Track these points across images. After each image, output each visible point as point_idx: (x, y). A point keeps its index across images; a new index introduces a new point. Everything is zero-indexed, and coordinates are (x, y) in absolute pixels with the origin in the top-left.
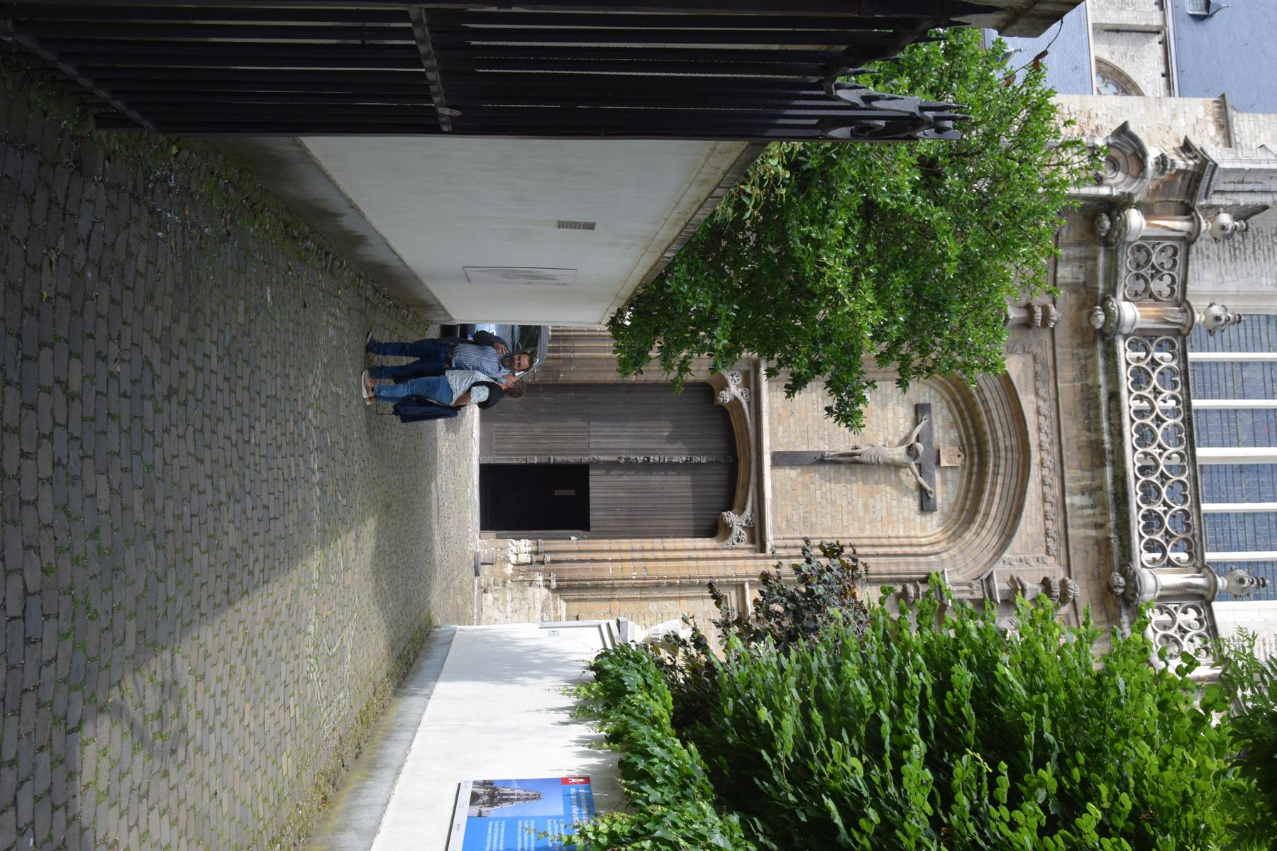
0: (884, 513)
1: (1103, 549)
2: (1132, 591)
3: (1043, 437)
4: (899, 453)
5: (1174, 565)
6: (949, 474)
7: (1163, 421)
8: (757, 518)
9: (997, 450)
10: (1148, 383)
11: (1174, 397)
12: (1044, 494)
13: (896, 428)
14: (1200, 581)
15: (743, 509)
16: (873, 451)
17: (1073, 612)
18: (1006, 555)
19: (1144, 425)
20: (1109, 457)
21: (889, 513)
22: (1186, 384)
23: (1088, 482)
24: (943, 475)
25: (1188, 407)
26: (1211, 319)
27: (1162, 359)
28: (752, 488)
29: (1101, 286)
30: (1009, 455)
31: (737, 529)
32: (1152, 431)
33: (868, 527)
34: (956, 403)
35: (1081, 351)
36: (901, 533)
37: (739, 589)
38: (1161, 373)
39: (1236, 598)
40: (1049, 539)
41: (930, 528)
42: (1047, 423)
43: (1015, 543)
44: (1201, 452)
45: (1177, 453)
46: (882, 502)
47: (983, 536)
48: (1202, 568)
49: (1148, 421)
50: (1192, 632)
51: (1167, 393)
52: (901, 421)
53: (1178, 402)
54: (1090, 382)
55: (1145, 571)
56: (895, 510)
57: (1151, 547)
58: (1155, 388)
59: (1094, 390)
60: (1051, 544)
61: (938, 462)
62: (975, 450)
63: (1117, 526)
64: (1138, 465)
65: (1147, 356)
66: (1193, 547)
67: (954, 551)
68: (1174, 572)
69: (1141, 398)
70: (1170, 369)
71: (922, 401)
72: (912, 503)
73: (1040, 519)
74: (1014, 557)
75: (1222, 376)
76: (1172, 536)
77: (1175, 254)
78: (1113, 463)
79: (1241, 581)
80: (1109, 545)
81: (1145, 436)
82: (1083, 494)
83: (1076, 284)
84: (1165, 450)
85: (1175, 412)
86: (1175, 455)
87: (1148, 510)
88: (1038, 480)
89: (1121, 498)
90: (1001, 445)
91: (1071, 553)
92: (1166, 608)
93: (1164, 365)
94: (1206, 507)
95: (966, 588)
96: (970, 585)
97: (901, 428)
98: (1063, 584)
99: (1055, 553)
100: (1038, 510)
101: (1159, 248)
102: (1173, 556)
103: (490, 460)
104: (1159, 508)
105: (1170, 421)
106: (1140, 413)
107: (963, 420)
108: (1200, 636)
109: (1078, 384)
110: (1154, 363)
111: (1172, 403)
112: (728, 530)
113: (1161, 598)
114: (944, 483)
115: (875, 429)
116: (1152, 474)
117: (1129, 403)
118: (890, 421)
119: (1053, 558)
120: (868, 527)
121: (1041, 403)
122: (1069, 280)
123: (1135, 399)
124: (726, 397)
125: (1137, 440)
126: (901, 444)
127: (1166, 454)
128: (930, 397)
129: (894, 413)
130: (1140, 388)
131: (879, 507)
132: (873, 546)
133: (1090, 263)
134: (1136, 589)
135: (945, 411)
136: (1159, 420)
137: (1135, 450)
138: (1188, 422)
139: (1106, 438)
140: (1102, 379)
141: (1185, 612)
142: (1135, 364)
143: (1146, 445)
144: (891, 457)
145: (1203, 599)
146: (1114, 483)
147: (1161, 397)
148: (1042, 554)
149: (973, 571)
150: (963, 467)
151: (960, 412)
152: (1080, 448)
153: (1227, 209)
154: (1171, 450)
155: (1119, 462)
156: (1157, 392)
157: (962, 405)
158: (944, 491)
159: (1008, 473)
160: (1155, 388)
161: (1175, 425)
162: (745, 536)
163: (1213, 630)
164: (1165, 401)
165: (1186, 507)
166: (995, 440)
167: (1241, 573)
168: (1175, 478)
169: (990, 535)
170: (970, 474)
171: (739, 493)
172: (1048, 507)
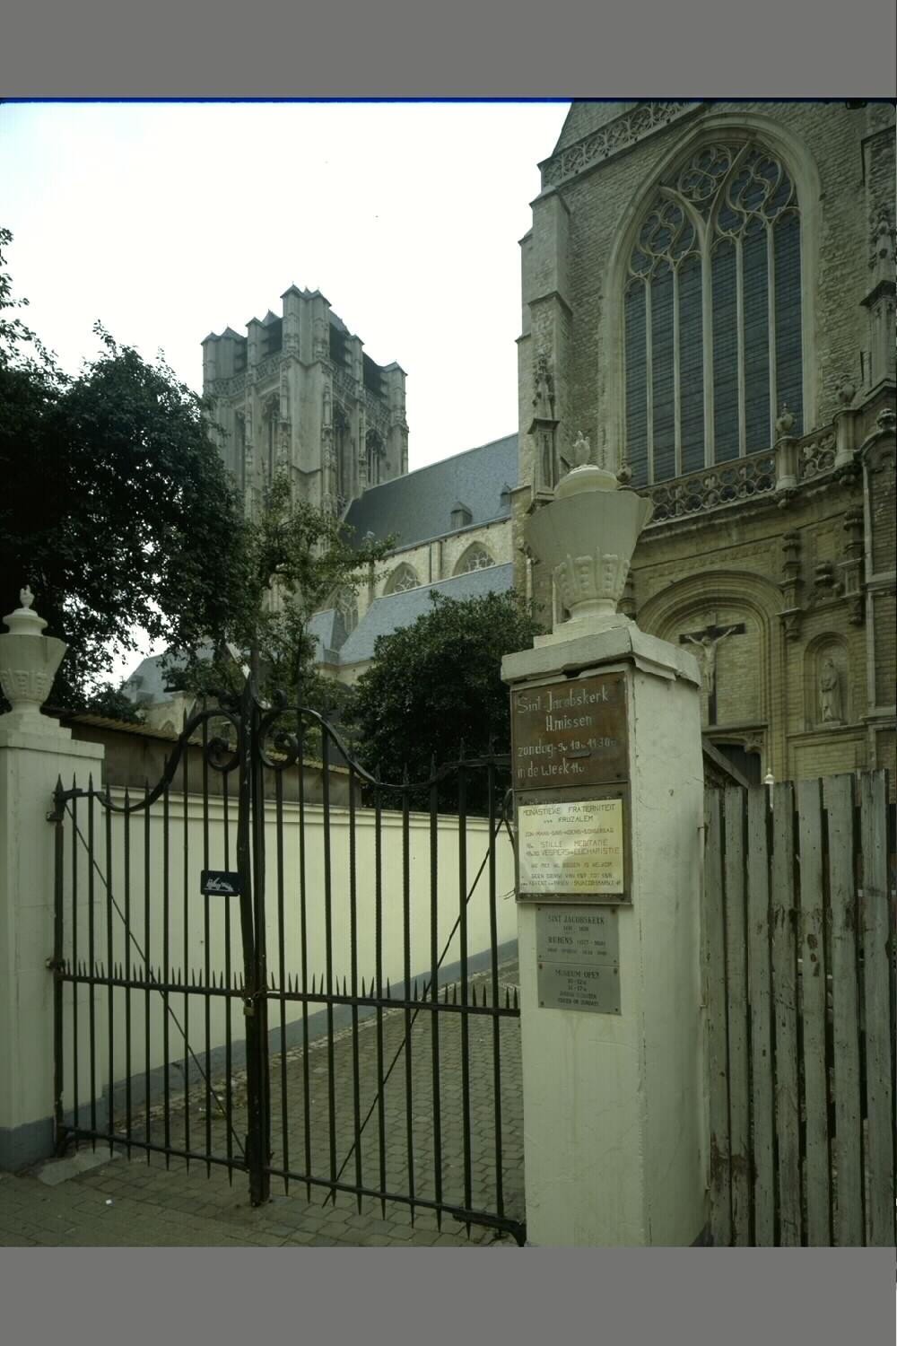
6: (722, 619)
9: (705, 593)
15: (742, 740)
24: (721, 622)
31: (755, 744)
61: (713, 627)
71: (678, 640)
72: (738, 639)
90: (701, 590)
98: (786, 538)
107: (689, 614)
114: (726, 621)
135: (685, 626)
155: (714, 515)
158: (732, 618)
166: (699, 594)
170: (720, 606)
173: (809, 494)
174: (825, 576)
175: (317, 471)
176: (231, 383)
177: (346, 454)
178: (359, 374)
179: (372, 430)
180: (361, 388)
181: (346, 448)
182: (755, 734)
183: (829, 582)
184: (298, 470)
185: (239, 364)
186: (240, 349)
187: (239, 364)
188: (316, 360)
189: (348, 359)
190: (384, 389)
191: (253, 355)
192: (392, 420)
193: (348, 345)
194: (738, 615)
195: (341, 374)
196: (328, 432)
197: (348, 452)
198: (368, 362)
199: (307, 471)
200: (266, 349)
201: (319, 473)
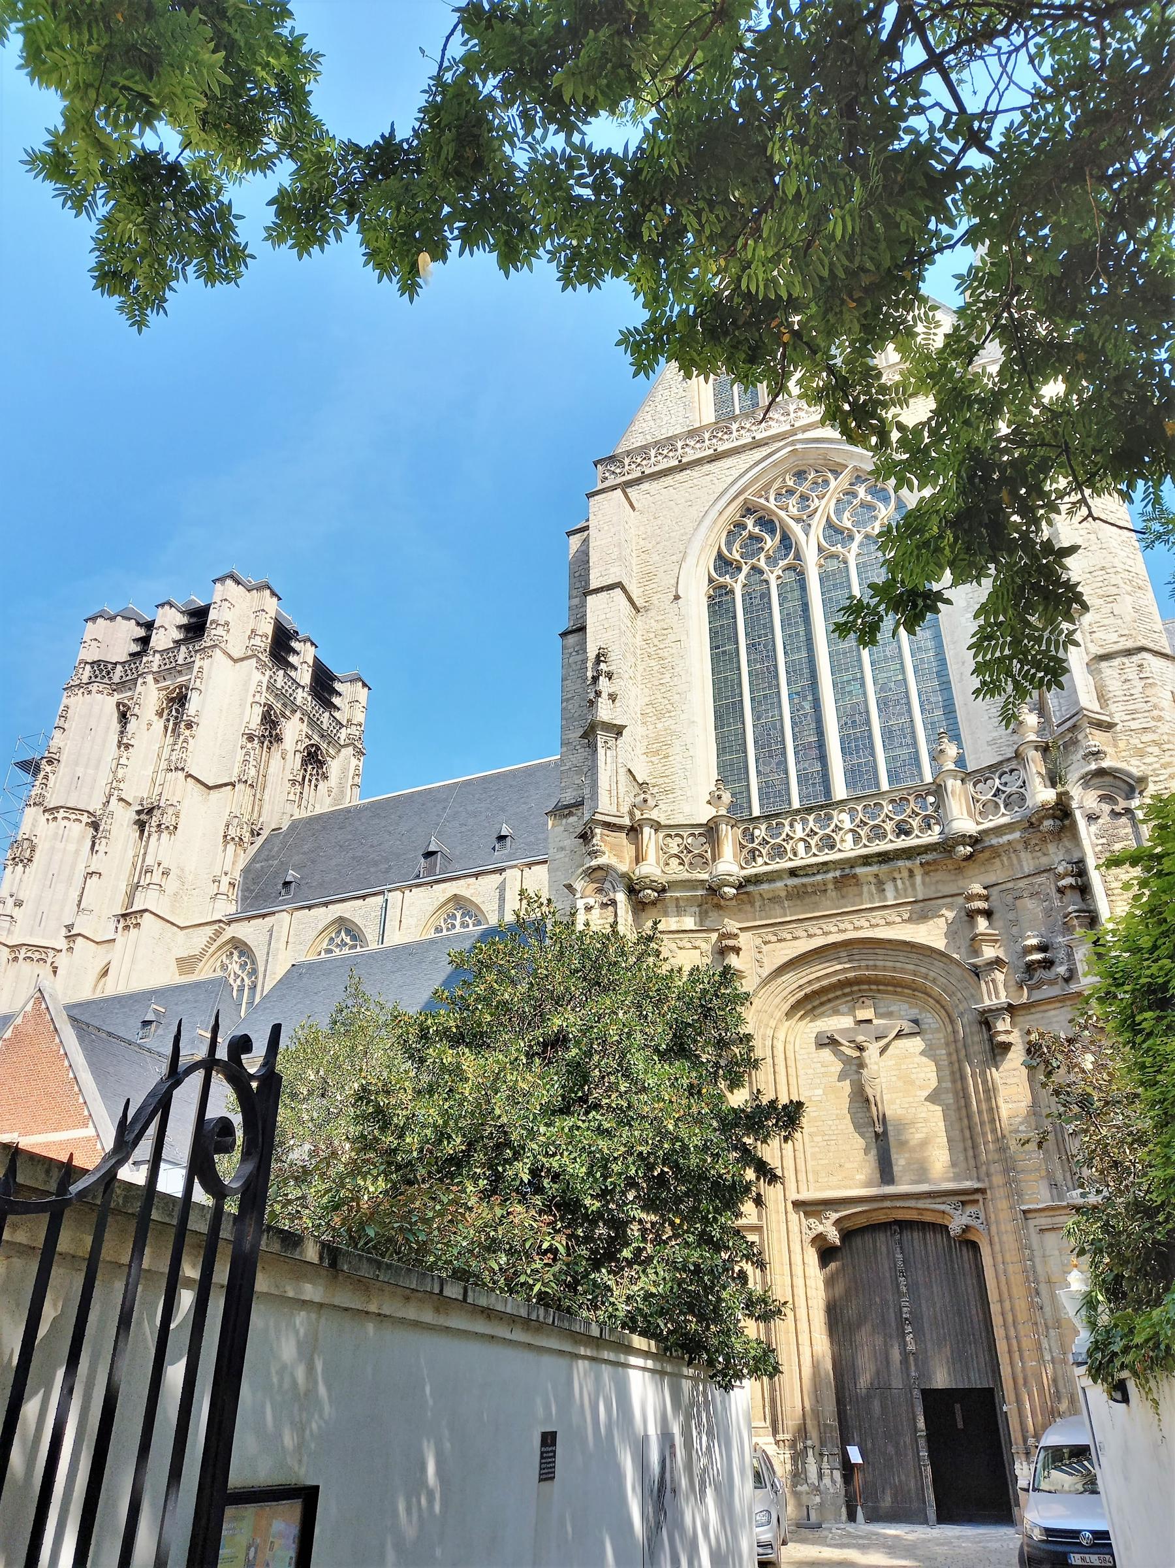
1: (932, 868)
2: (968, 840)
8: (951, 1198)
17: (996, 888)
20: (847, 871)
22: (777, 815)
23: (873, 887)
25: (798, 811)
28: (921, 1204)
29: (700, 893)
30: (857, 957)
34: (814, 1008)
35: (757, 904)
37: (1029, 1216)
51: (787, 829)
54: (783, 894)
59: (790, 889)
62: (855, 988)
63: (909, 858)
77: (670, 836)
78: (852, 867)
80: (927, 863)
82: (884, 890)
83: (700, 913)
89: (884, 858)
91: (940, 895)
94: (885, 786)
103: (932, 1513)
107: (829, 1001)
109: (786, 903)
112: (967, 1229)
122: (698, 919)
123: (795, 854)
124: (834, 1236)
133: (681, 903)
136: (813, 833)
139: (830, 875)
140: (779, 884)
146: (870, 865)
150: (874, 998)
151: (822, 1004)
152: (843, 897)
155: (852, 863)
159: (874, 957)
162: (970, 1209)
166: (844, 970)
170: (879, 991)
171: (928, 1218)
173: (994, 841)
176: (119, 667)
177: (271, 770)
179: (312, 745)
180: (305, 695)
182: (963, 1203)
183: (1048, 964)
186: (141, 632)
187: (135, 648)
188: (250, 653)
189: (293, 659)
194: (906, 1006)
195: (281, 673)
196: (251, 738)
200: (179, 635)
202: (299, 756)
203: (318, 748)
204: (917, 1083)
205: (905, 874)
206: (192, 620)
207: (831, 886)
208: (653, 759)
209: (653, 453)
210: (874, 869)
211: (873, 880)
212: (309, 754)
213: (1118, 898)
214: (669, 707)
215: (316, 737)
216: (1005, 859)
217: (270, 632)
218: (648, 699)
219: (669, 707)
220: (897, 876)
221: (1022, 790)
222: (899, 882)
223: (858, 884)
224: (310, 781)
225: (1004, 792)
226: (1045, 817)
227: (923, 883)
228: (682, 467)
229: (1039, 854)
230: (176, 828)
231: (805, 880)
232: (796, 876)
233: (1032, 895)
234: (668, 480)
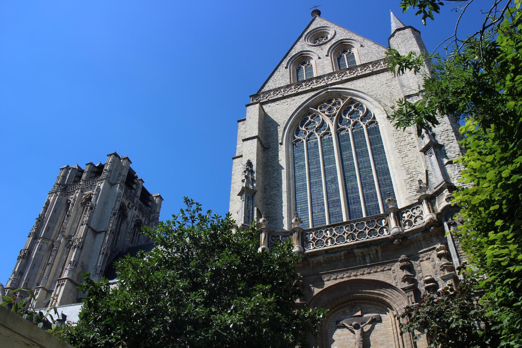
0: (384, 336)
3: (345, 276)
4: (358, 332)
5: (388, 223)
7: (334, 234)
10: (321, 240)
11: (326, 232)
12: (367, 273)
13: (348, 335)
14: (392, 214)
16: (358, 343)
18: (394, 284)
19: (337, 240)
21: (383, 334)
25: (328, 226)
26: (297, 223)
27: (312, 237)
32: (338, 237)
33: (390, 343)
36: (391, 328)
38: (317, 237)
39: (396, 201)
40: (385, 269)
41: (388, 318)
42: (339, 275)
43: (389, 282)
44: (345, 220)
45: (346, 228)
46: (379, 338)
47: (389, 296)
48: (387, 215)
49: (335, 239)
50: (411, 213)
51: (324, 234)
52: (344, 332)
53: (328, 230)
55: (391, 233)
56: (382, 332)
57: (381, 231)
58: (323, 238)
60: (387, 269)
64: (352, 240)
65: (311, 242)
66: (380, 218)
67: (396, 306)
68: (390, 223)
69: (327, 242)
70: (315, 234)
73: (377, 274)
74: (394, 282)
75: (318, 219)
76: (377, 226)
77: (274, 236)
79: (389, 200)
81: (341, 238)
82: (365, 259)
84: (345, 232)
85: (331, 231)
86: (347, 229)
87: (368, 235)
88: (362, 276)
92: (404, 224)
93: (314, 236)
95: (410, 298)
96: (408, 297)
97: (347, 332)
99: (390, 266)
100: (374, 275)
101: (272, 242)
102: (384, 224)
104: (367, 231)
105: (334, 231)
106: (332, 242)
108: (412, 211)
110: (314, 239)
111: (328, 232)
113: (400, 226)
115: (348, 343)
116: (355, 235)
117: (329, 246)
118: (345, 337)
119: (392, 267)
120: (390, 343)
121: (332, 278)
125: (342, 242)
126: (353, 332)
127: (346, 231)
128: (333, 322)
129: (341, 336)
130: (323, 243)
131: (382, 339)
132: (398, 340)
134: (398, 234)
137: (346, 242)
138: (334, 226)
139: (342, 253)
141: (404, 217)
142: (315, 246)
143: (344, 239)
144: (359, 335)
145: (398, 214)
147: (326, 235)
148: (391, 271)
149: (402, 297)
151: (339, 309)
153: (258, 220)
154: (345, 230)
156: (324, 237)
157: (336, 309)
160: (323, 238)
161: (335, 230)
163: (409, 207)
164: (327, 234)
165: (365, 223)
167: (386, 201)
168: (355, 227)
169: (387, 292)
172: (372, 271)
174: (432, 284)
175: (103, 231)
177: (122, 228)
178: (139, 193)
179: (139, 220)
180: (138, 200)
181: (123, 225)
184: (92, 230)
185: (77, 179)
189: (134, 186)
190: (150, 203)
191: (84, 176)
192: (151, 218)
193: (135, 181)
196: (114, 214)
197: (124, 227)
198: (144, 190)
199: (98, 230)
201: (104, 233)
202: (133, 224)
203: (141, 221)
204: (379, 342)
205: (374, 252)
206: (98, 170)
207: (343, 258)
208: (268, 206)
209: (272, 93)
210: (361, 250)
211: (361, 255)
212: (137, 223)
213: (463, 257)
214: (276, 186)
215: (140, 217)
216: (415, 244)
217: (126, 175)
218: (267, 183)
219: (276, 186)
220: (371, 253)
221: (421, 215)
222: (372, 256)
223: (355, 256)
224: (137, 234)
225: (414, 216)
226: (432, 226)
227: (382, 255)
228: (284, 98)
229: (429, 242)
230: (82, 247)
231: (332, 255)
232: (328, 253)
233: (427, 259)
234: (278, 102)
